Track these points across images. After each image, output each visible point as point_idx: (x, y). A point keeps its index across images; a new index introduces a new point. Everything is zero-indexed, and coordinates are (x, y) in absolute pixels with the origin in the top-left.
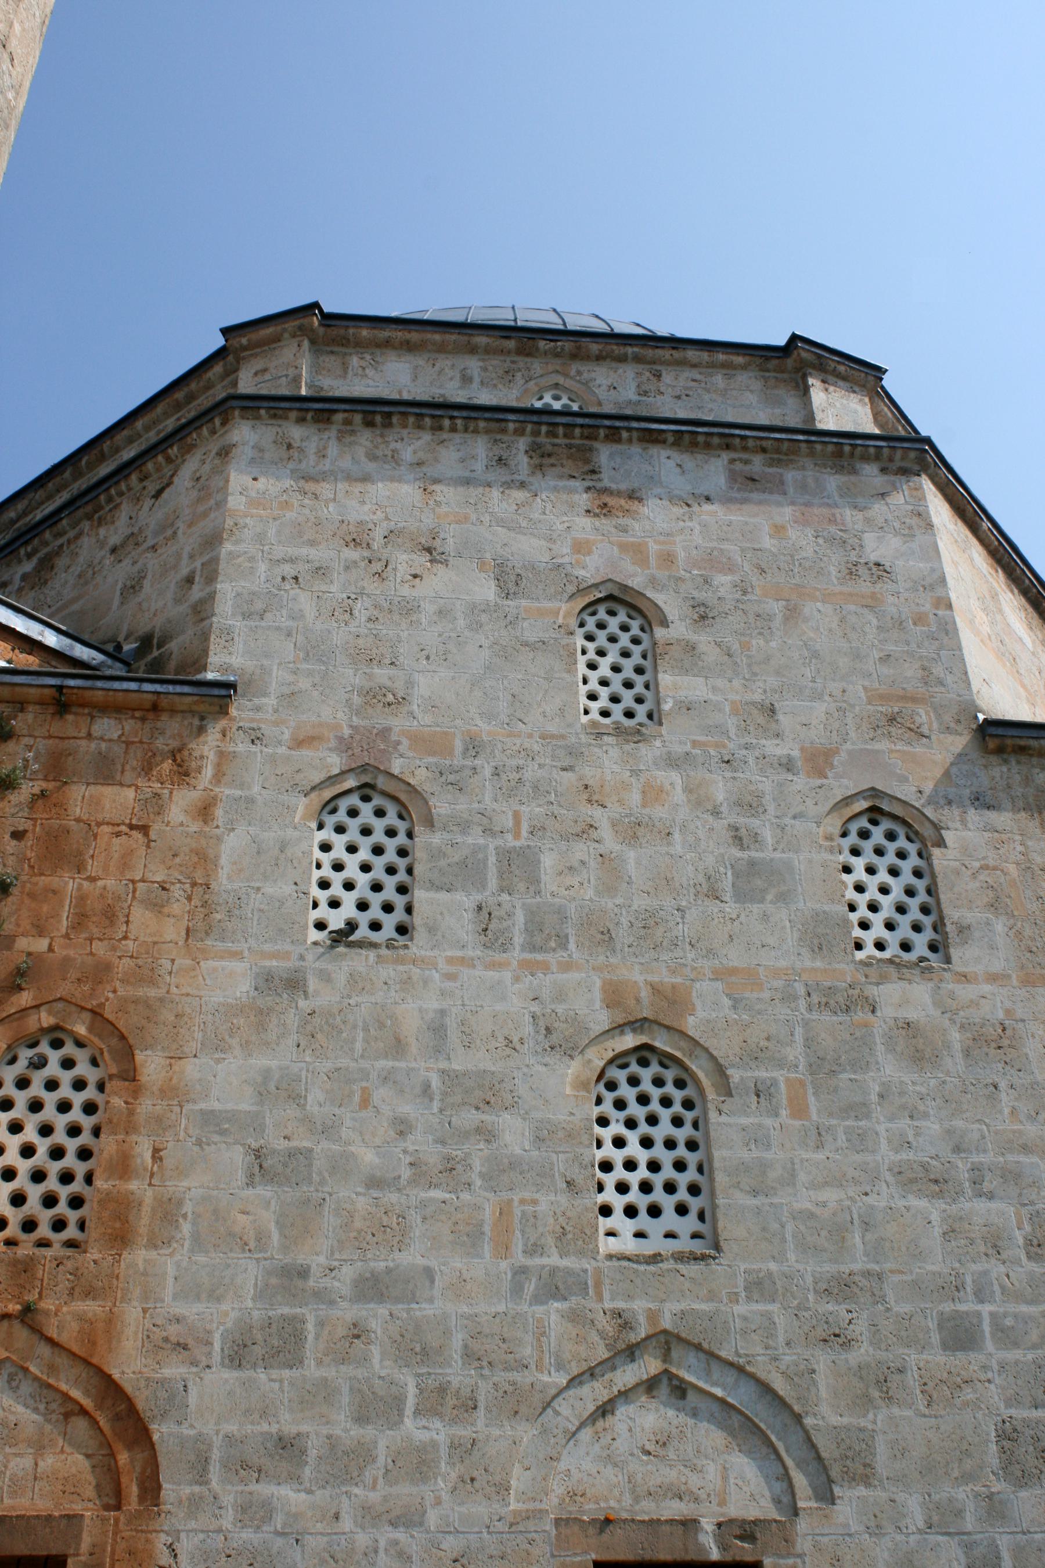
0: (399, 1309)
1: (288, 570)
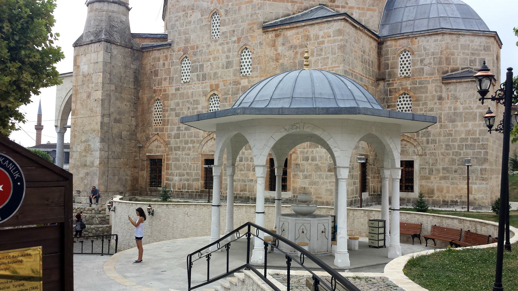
1: (176, 19)
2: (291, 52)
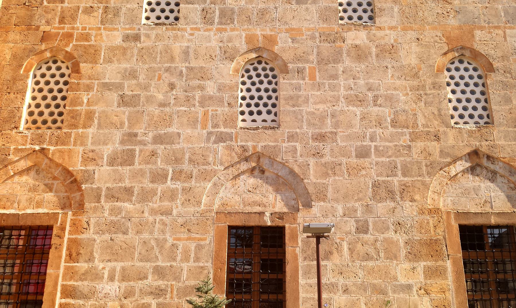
0: (168, 147)
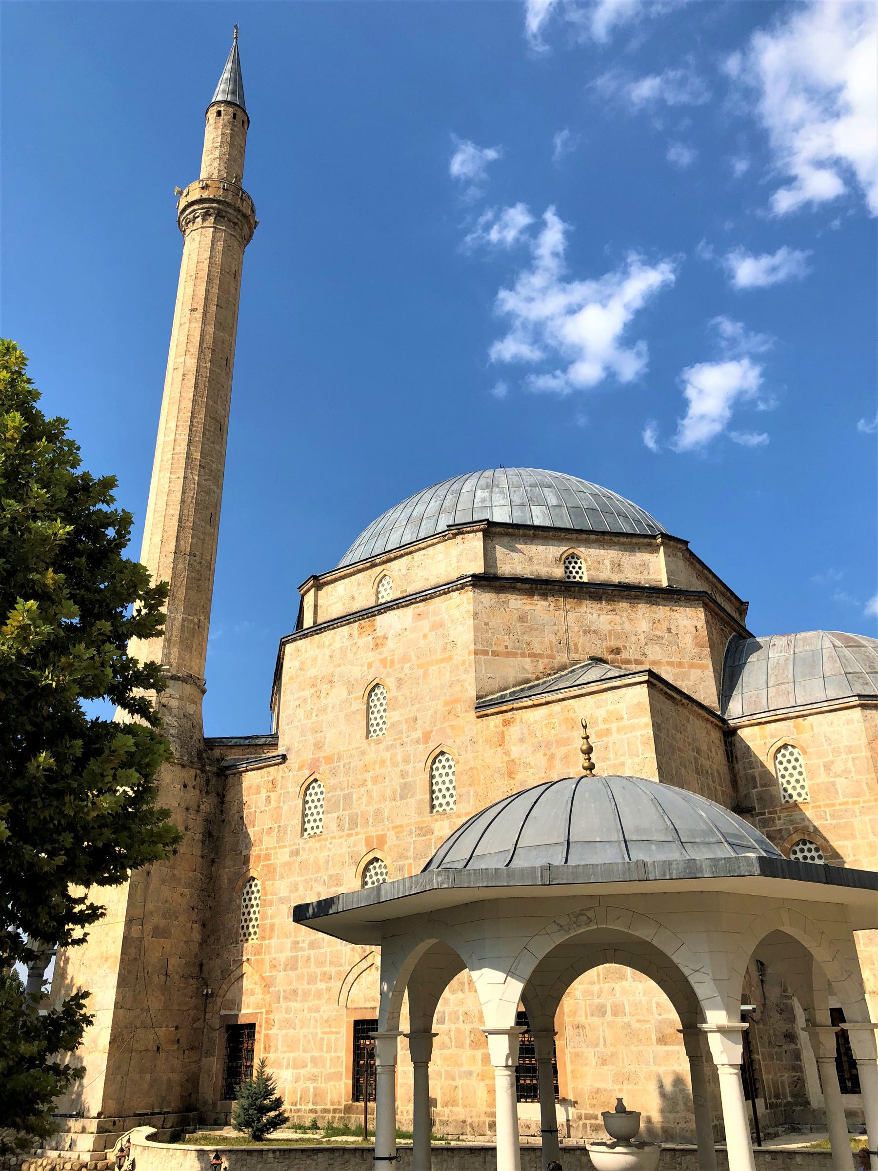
1: (297, 703)
2: (540, 755)
